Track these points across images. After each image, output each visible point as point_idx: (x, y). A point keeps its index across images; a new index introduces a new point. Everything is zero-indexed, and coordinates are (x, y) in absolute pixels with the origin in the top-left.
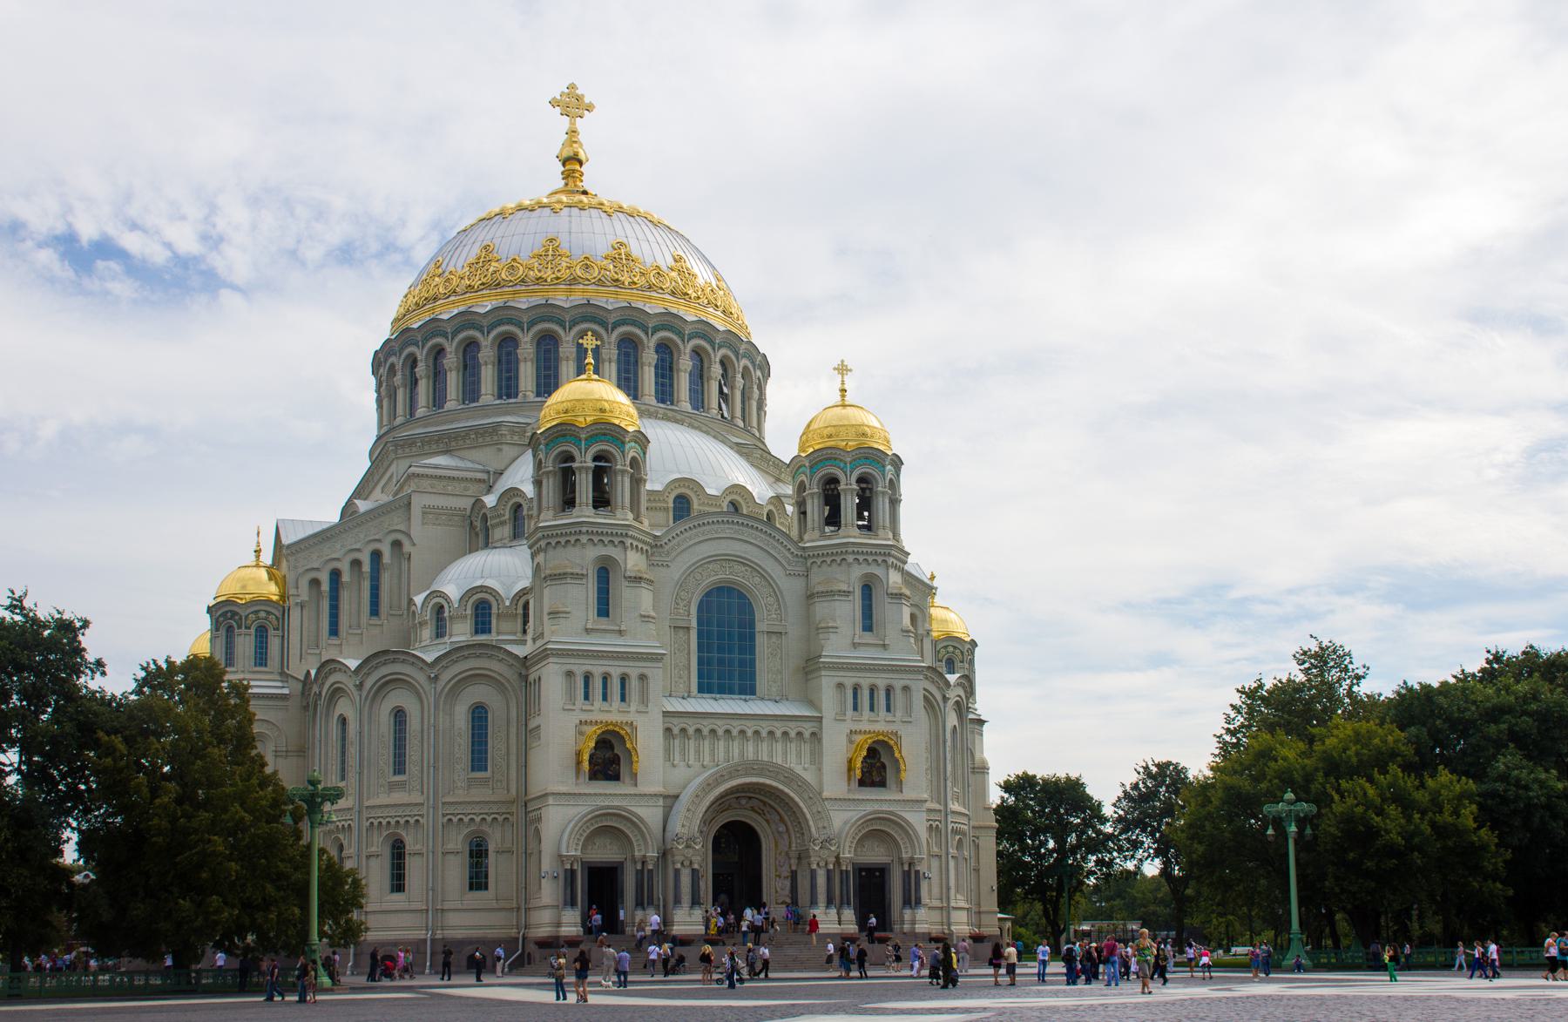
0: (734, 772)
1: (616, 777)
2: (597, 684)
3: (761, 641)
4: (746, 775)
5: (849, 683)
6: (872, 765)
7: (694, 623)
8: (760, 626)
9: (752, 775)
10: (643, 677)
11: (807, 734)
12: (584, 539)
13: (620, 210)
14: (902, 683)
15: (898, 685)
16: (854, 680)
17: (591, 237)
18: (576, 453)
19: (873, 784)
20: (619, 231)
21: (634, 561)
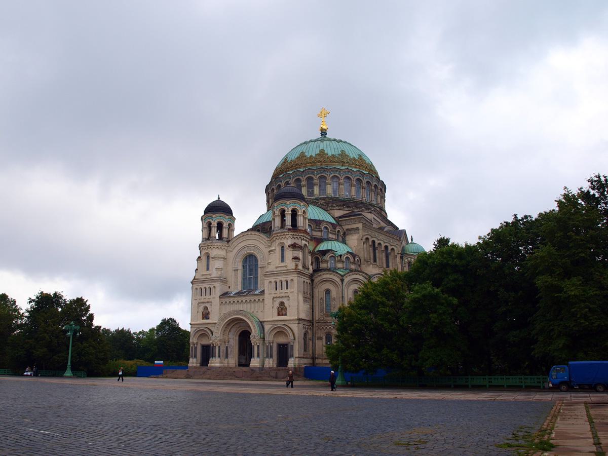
0: (229, 314)
1: (209, 319)
2: (204, 290)
3: (259, 269)
4: (230, 316)
5: (273, 281)
6: (282, 309)
7: (240, 267)
8: (259, 266)
9: (235, 315)
10: (214, 287)
11: (261, 300)
12: (212, 247)
13: (341, 141)
14: (291, 278)
15: (289, 279)
16: (275, 280)
17: (331, 150)
18: (212, 222)
19: (282, 315)
20: (342, 147)
21: (214, 252)
